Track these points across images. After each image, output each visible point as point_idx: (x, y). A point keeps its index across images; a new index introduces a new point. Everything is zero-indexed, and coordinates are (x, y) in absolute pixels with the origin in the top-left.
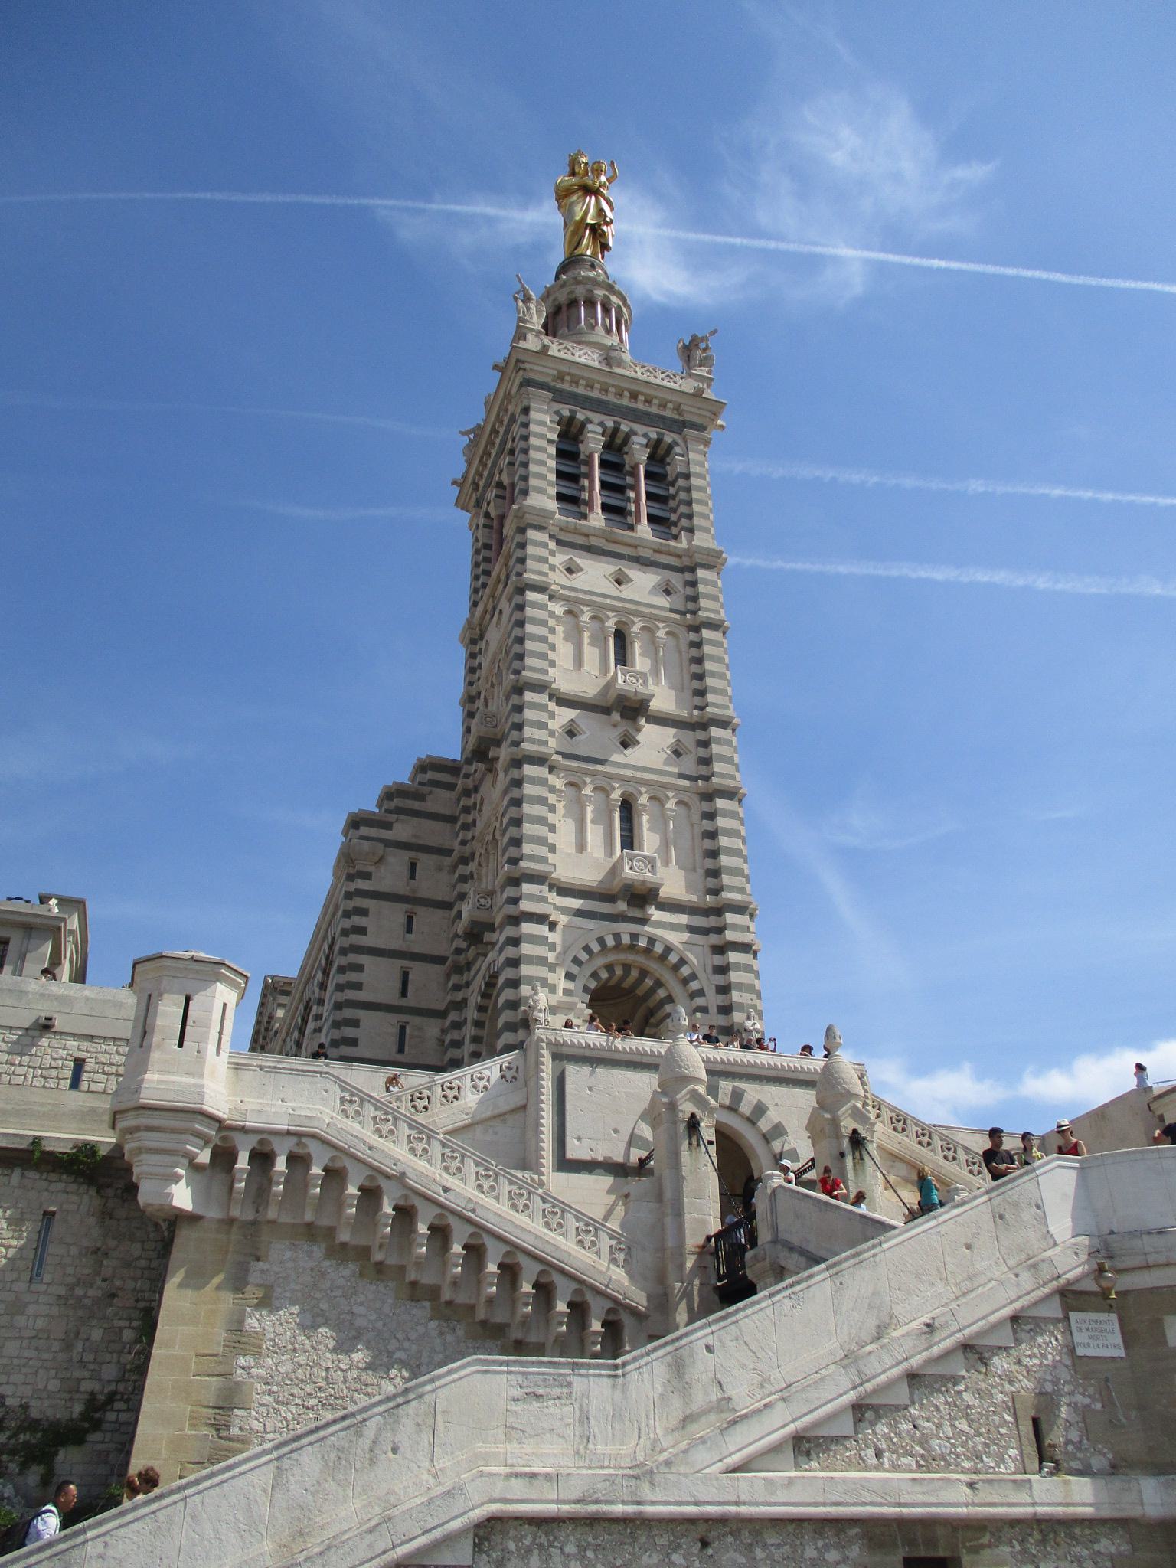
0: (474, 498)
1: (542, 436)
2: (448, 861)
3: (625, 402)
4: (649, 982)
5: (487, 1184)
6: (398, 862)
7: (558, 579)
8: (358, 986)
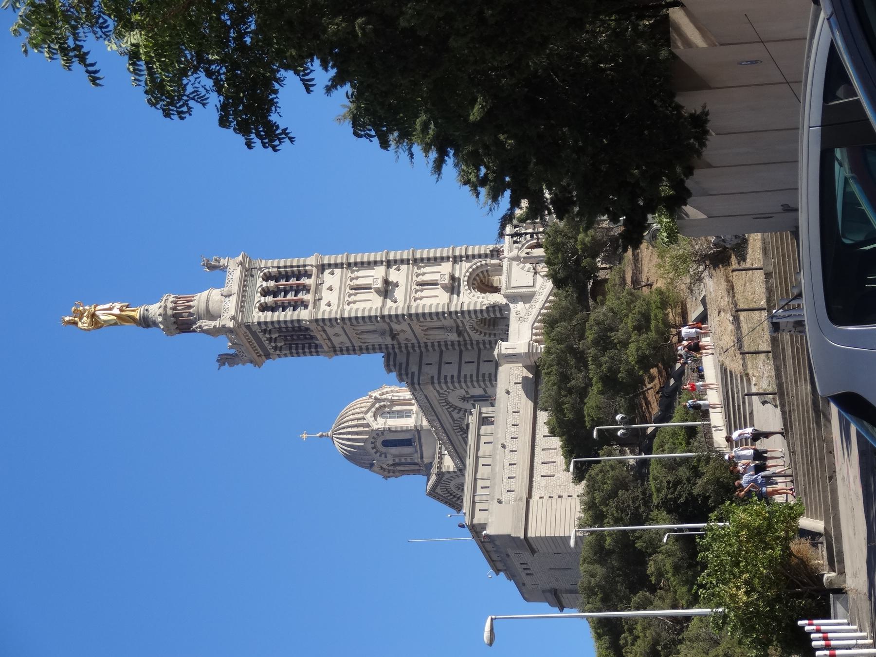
0: (263, 357)
1: (272, 317)
2: (424, 354)
4: (477, 278)
5: (541, 294)
6: (426, 369)
7: (334, 308)
8: (471, 376)
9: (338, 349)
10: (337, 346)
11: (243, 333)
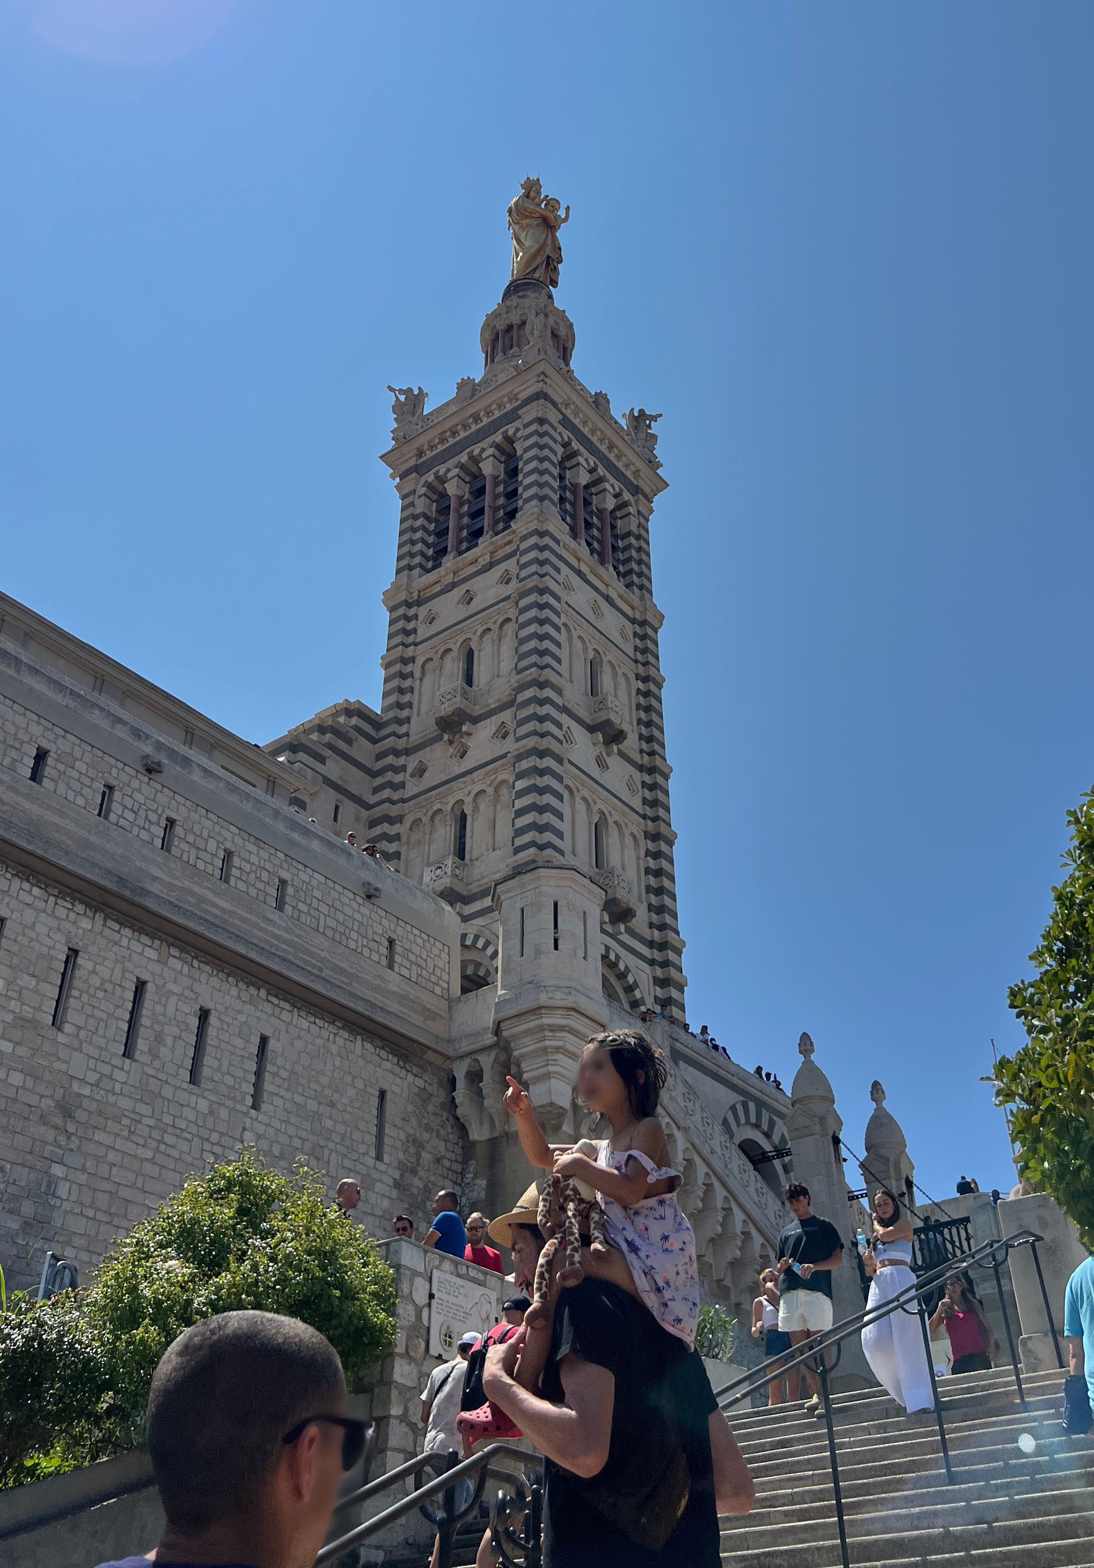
2: (364, 813)
3: (603, 448)
6: (330, 796)
9: (412, 612)
10: (422, 612)
11: (516, 391)
